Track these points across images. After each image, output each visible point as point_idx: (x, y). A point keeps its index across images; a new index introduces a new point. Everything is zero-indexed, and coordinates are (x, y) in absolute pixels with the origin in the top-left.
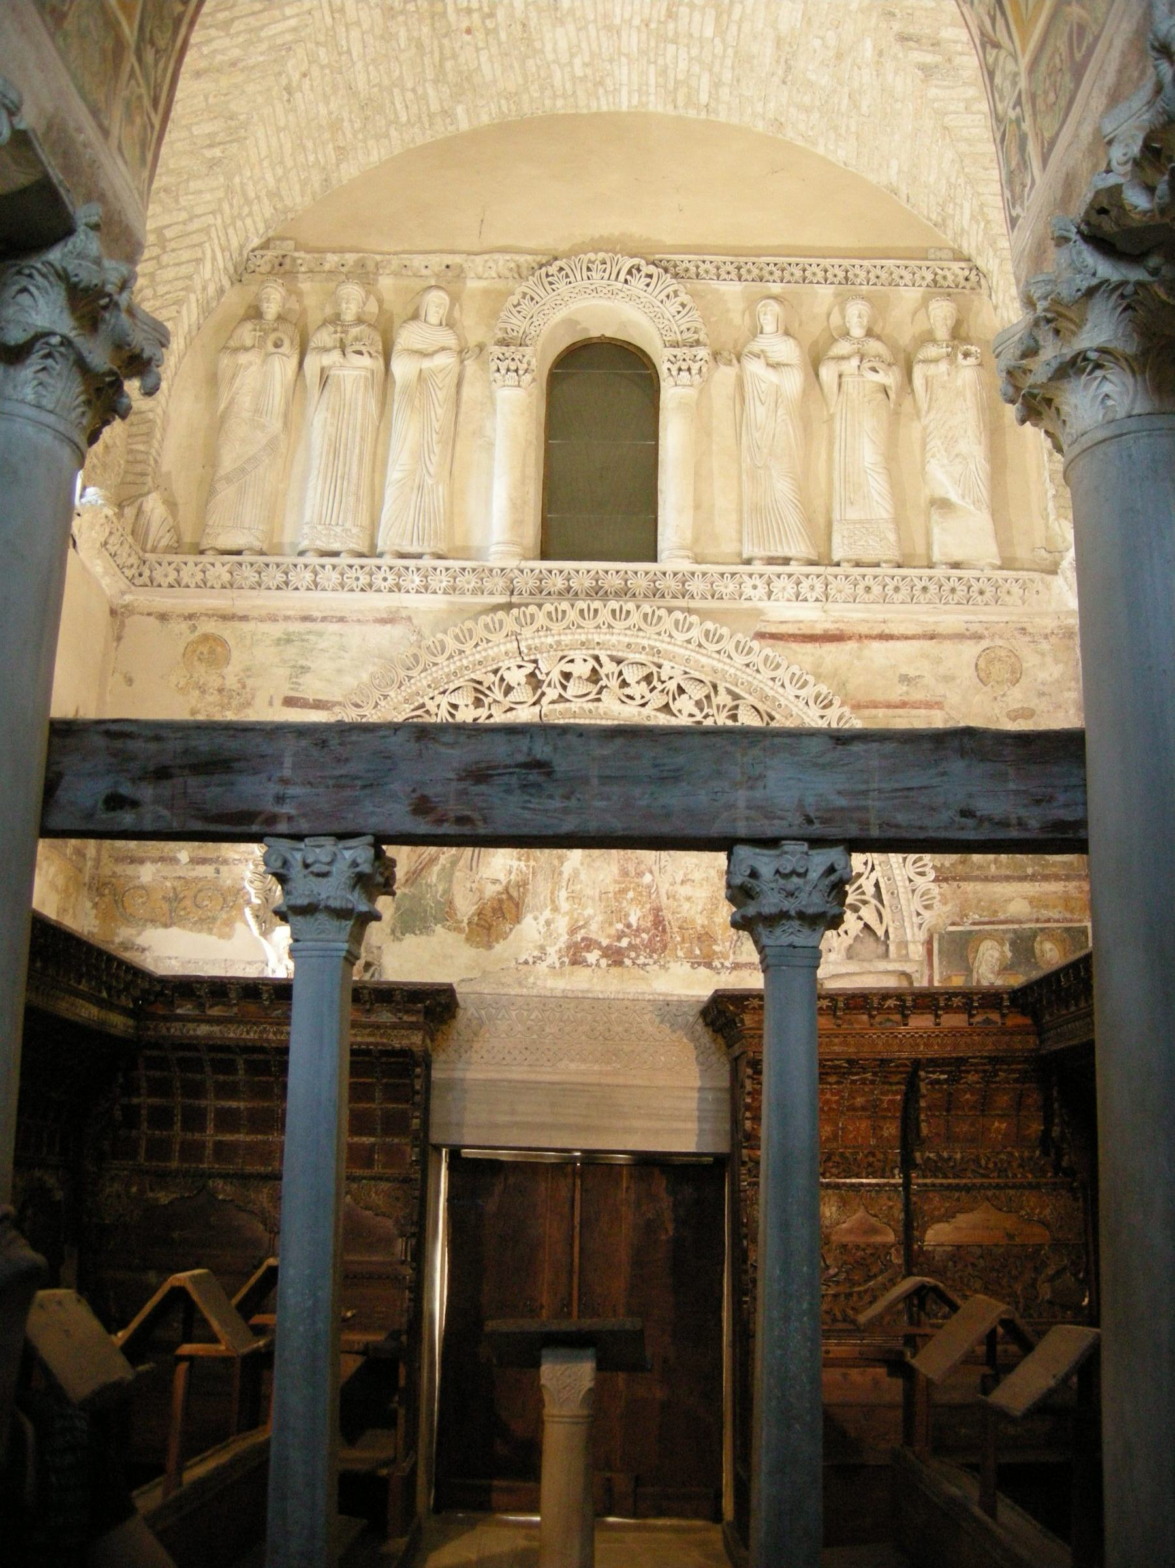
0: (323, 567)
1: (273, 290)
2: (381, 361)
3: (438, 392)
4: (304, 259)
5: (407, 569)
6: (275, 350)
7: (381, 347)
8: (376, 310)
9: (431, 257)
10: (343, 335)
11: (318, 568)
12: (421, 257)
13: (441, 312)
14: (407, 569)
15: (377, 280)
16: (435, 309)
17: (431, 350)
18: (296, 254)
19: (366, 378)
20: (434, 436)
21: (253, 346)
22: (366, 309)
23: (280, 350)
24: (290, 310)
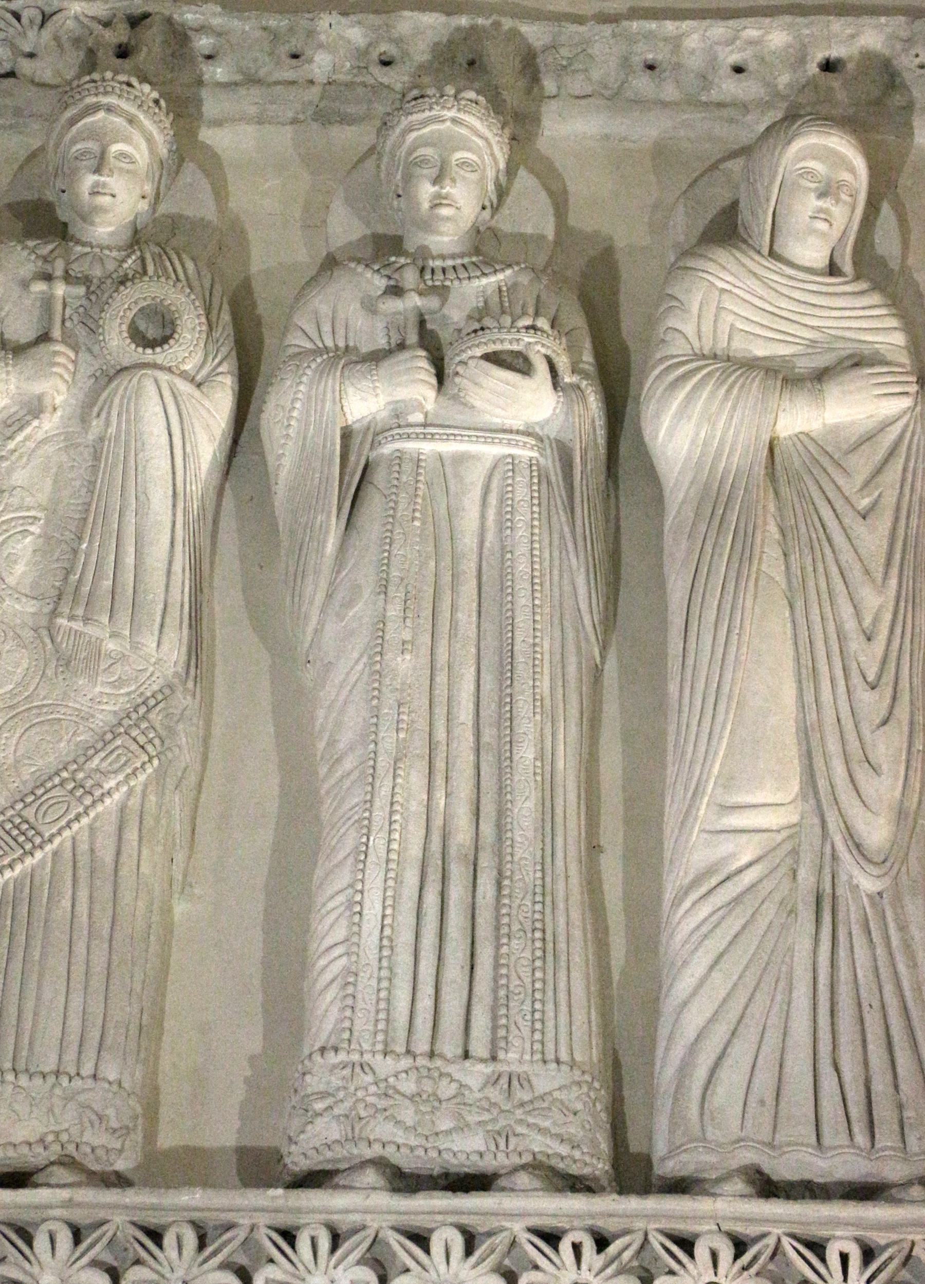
0: (421, 1239)
1: (118, 120)
2: (594, 402)
3: (859, 529)
4: (219, 34)
5: (817, 1247)
6: (134, 353)
7: (588, 357)
8: (550, 233)
9: (751, 31)
10: (433, 302)
11: (394, 1240)
12: (719, 30)
13: (839, 213)
14: (817, 1247)
15: (536, 120)
16: (813, 203)
17: (804, 365)
18: (190, 16)
19: (543, 477)
20: (865, 696)
21: (44, 338)
22: (505, 223)
23: (159, 356)
24: (174, 223)
